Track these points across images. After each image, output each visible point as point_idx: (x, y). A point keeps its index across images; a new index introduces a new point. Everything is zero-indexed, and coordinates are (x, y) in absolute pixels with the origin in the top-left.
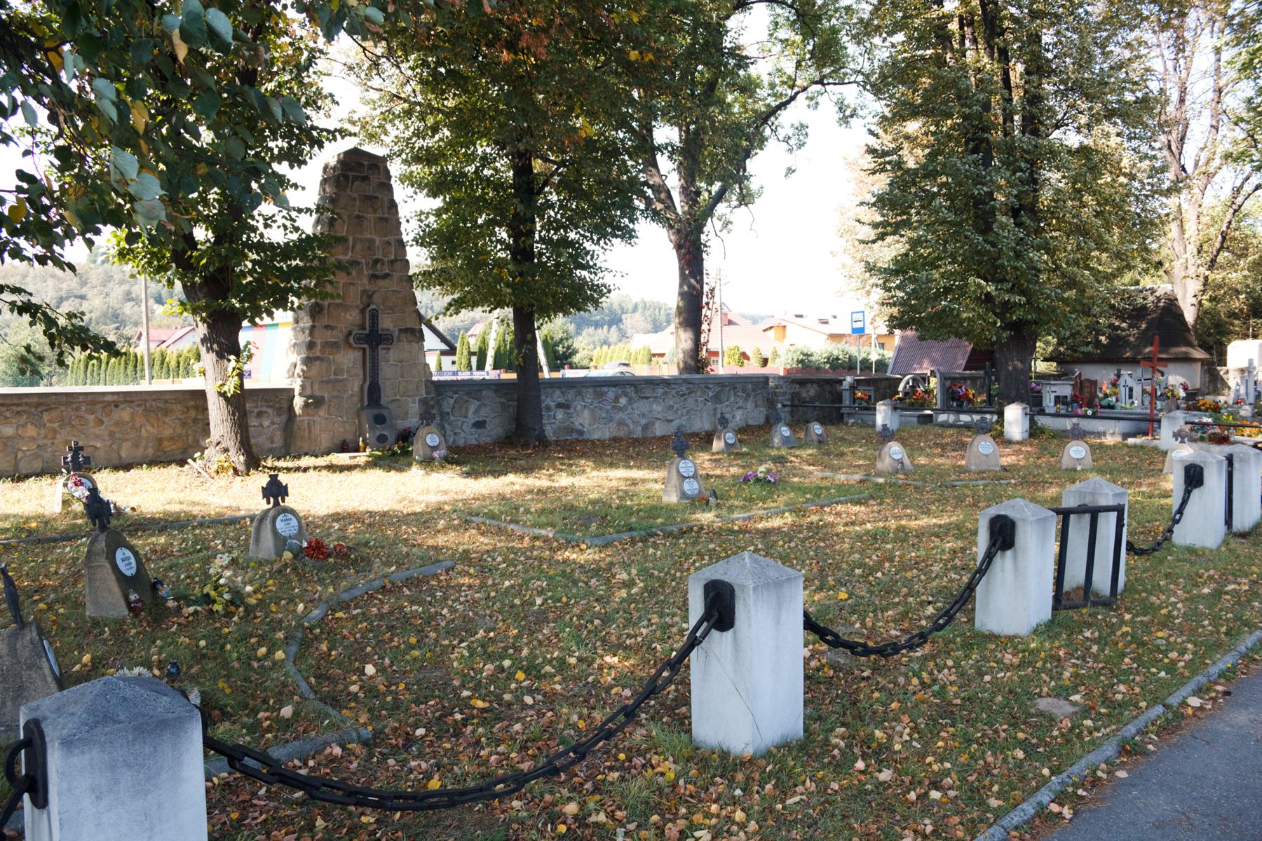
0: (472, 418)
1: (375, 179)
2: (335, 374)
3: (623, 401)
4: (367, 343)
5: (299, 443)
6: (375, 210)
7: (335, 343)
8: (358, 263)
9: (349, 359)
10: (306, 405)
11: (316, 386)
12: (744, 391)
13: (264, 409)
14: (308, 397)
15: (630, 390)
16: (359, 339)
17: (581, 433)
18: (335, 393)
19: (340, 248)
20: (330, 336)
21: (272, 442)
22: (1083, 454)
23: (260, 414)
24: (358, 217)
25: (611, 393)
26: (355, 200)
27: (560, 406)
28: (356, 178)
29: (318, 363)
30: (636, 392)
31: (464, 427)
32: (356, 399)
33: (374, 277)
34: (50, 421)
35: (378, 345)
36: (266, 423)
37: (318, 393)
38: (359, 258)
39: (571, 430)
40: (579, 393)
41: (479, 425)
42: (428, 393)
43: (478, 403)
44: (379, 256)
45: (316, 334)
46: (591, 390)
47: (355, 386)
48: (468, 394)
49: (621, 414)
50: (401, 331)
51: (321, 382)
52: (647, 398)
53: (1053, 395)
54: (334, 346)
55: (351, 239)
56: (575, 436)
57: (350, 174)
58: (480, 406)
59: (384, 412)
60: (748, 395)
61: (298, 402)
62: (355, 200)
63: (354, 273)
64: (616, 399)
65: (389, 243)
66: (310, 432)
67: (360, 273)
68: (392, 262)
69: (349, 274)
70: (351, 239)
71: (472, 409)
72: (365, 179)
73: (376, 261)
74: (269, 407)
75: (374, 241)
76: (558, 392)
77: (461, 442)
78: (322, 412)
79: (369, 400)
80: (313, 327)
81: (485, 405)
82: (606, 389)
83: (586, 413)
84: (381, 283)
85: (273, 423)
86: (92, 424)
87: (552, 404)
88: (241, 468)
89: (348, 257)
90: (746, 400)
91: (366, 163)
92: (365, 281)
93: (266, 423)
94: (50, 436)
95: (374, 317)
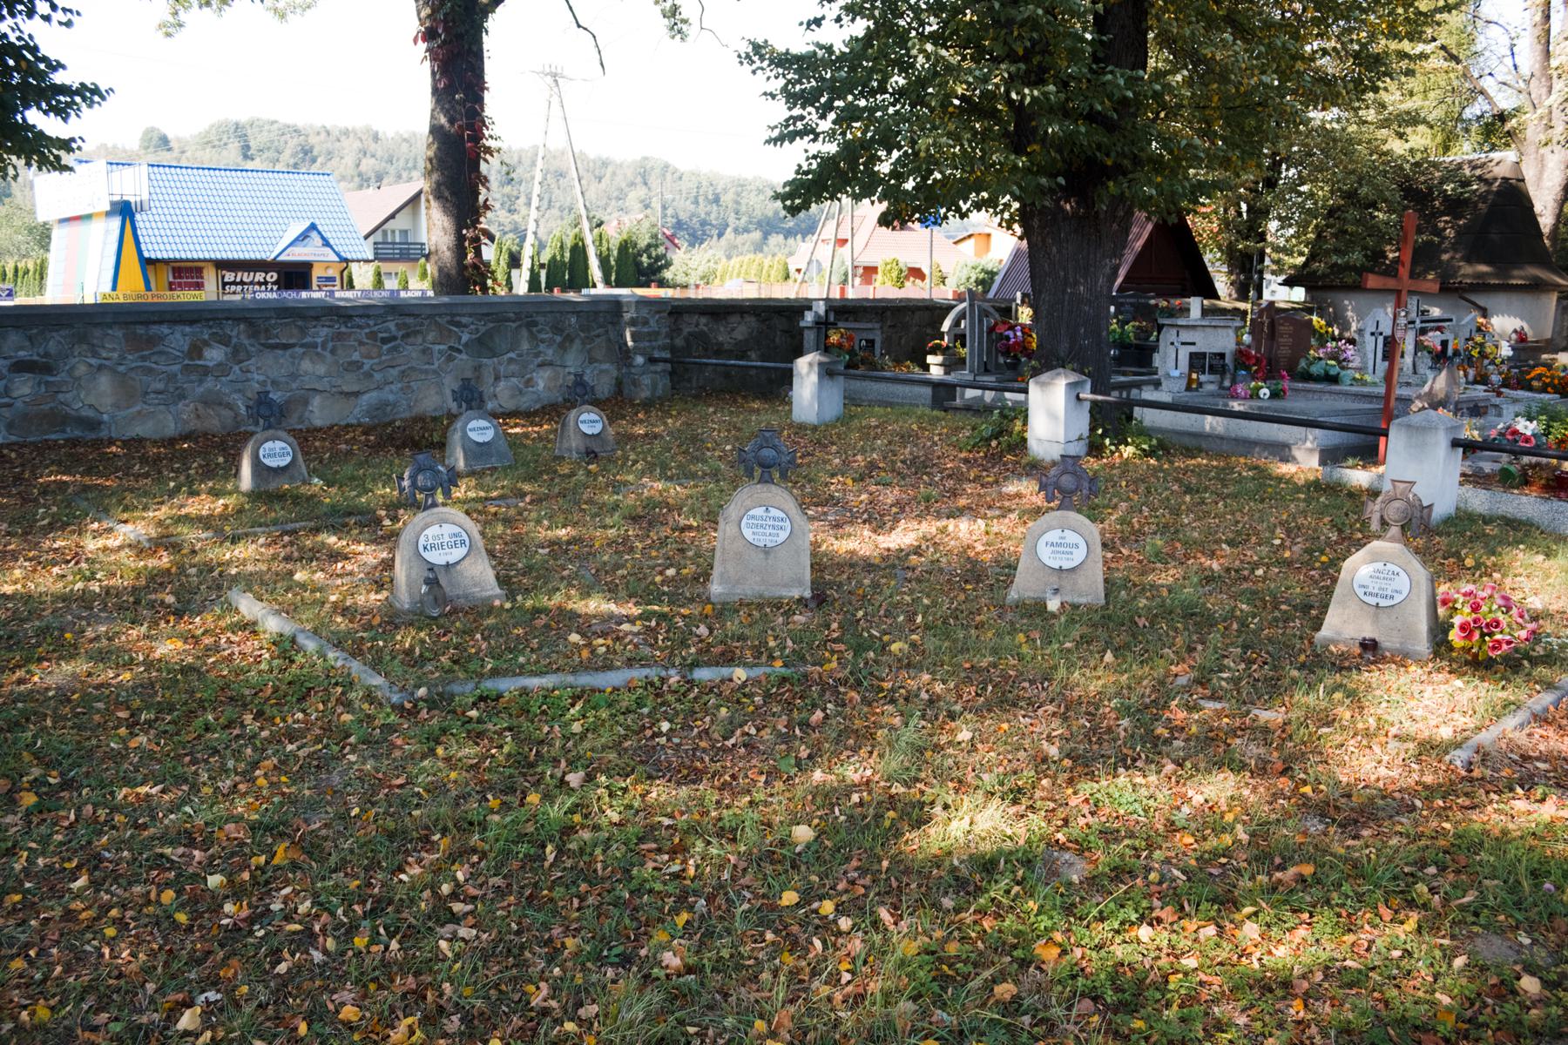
3: (214, 355)
12: (557, 329)
15: (238, 333)
17: (94, 425)
22: (1079, 556)
25: (178, 339)
30: (254, 335)
39: (59, 419)
40: (82, 339)
46: (119, 333)
52: (286, 347)
53: (1184, 353)
56: (74, 432)
60: (569, 339)
64: (196, 351)
82: (165, 329)
83: (104, 382)
90: (563, 347)
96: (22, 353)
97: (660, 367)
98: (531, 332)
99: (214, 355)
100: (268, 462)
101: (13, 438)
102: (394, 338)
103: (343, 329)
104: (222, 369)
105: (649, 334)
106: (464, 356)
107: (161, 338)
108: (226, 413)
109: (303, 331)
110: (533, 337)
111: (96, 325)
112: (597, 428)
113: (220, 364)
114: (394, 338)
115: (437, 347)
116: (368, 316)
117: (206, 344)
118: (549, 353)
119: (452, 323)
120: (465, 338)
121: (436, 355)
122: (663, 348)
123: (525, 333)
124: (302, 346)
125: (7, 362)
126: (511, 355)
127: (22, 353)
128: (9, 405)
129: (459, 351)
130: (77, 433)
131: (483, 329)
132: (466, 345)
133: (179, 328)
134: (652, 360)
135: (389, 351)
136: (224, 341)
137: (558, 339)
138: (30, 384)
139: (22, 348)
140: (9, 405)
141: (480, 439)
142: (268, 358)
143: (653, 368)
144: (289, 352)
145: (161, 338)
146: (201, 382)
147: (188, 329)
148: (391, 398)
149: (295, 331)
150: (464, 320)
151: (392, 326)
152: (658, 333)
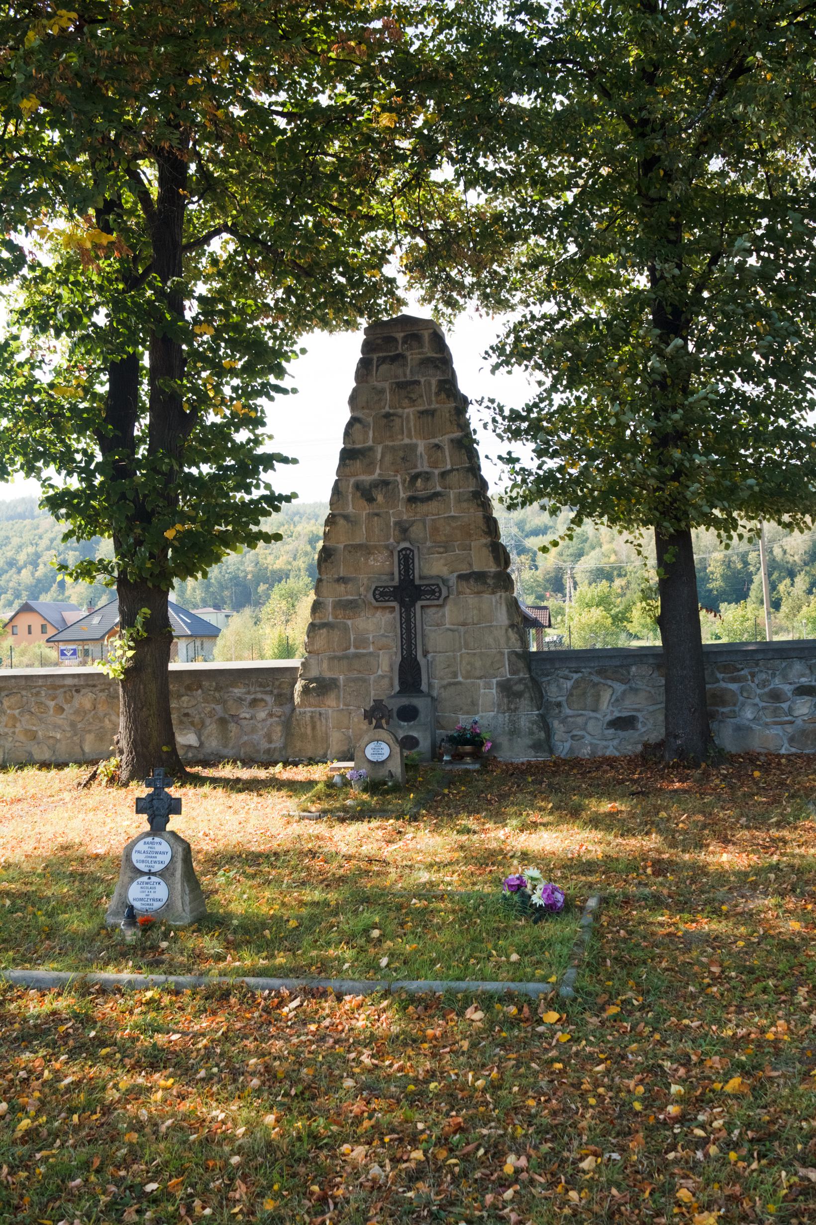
0: (607, 709)
1: (413, 356)
2: (356, 648)
5: (298, 744)
6: (413, 402)
7: (351, 602)
10: (306, 690)
11: (325, 665)
13: (259, 696)
14: (311, 681)
16: (382, 594)
18: (355, 675)
19: (358, 464)
20: (345, 593)
21: (270, 741)
23: (254, 703)
24: (387, 416)
26: (382, 391)
28: (382, 361)
31: (591, 726)
32: (385, 682)
33: (412, 500)
34: (9, 707)
35: (413, 603)
36: (262, 715)
37: (328, 675)
38: (390, 475)
41: (623, 723)
42: (512, 672)
43: (620, 688)
44: (423, 466)
45: (325, 591)
48: (601, 672)
50: (461, 577)
51: (332, 659)
54: (349, 607)
55: (379, 449)
57: (375, 356)
58: (624, 693)
59: (419, 703)
61: (298, 687)
62: (382, 391)
63: (380, 498)
65: (437, 447)
66: (314, 728)
67: (391, 497)
68: (443, 475)
69: (371, 500)
70: (379, 449)
71: (606, 697)
72: (397, 358)
73: (415, 478)
74: (266, 693)
75: (413, 448)
76: (798, 667)
77: (585, 752)
78: (331, 701)
79: (401, 683)
81: (635, 691)
84: (423, 508)
85: (271, 715)
86: (52, 712)
87: (787, 689)
88: (124, 775)
89: (375, 476)
91: (400, 336)
92: (401, 507)
93: (262, 715)
94: (10, 724)
95: (406, 560)
96: (803, 680)
101: (793, 750)
125: (792, 687)
127: (803, 680)
128: (792, 723)
138: (808, 705)
139: (803, 676)
140: (792, 723)
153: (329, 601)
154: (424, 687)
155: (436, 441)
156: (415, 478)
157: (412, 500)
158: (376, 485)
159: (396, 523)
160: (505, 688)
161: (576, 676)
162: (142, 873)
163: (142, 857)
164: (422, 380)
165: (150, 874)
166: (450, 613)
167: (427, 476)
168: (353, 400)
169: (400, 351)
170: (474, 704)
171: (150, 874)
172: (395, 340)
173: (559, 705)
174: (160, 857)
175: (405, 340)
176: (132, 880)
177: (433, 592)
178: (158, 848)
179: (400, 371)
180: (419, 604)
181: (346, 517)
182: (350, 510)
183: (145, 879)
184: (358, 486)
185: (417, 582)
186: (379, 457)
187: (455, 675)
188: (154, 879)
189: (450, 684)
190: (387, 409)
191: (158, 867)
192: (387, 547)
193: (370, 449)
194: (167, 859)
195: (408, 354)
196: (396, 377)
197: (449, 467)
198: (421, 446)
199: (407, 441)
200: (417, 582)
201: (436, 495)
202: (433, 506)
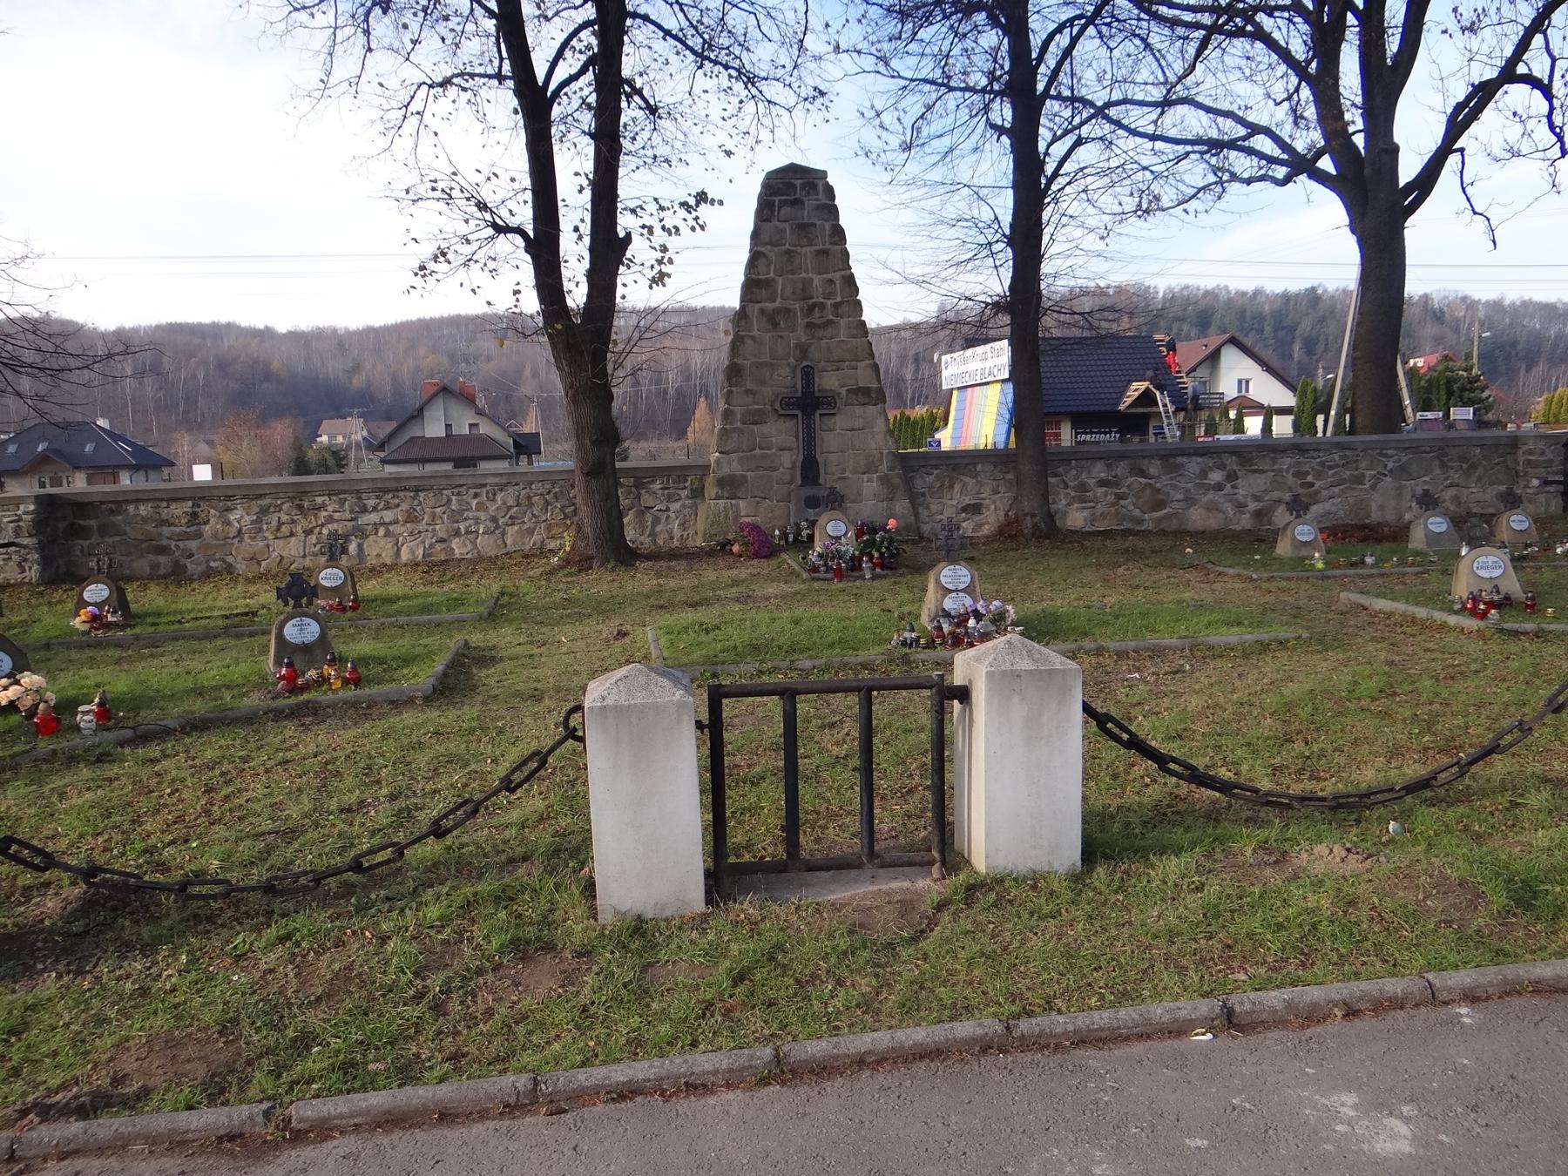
1: (810, 203)
4: (799, 409)
8: (789, 310)
9: (781, 434)
12: (1463, 459)
15: (1232, 463)
19: (764, 293)
24: (788, 252)
25: (1193, 465)
27: (1102, 483)
28: (783, 203)
29: (735, 435)
35: (813, 412)
47: (789, 460)
49: (1211, 495)
52: (1262, 472)
55: (780, 281)
57: (777, 199)
60: (1474, 467)
64: (1204, 474)
65: (831, 281)
68: (836, 306)
72: (797, 203)
73: (811, 308)
79: (803, 478)
80: (730, 392)
82: (1184, 460)
90: (1467, 474)
91: (798, 183)
95: (808, 375)
97: (1552, 488)
98: (1441, 461)
99: (1216, 476)
100: (1299, 538)
102: (1338, 466)
103: (1301, 459)
104: (1219, 487)
105: (1544, 462)
106: (1388, 479)
107: (1182, 466)
108: (1221, 516)
109: (1274, 461)
110: (1443, 465)
111: (1144, 457)
112: (1525, 526)
113: (1218, 483)
114: (1338, 466)
115: (1368, 473)
116: (1319, 450)
117: (1211, 469)
118: (1456, 477)
119: (1381, 454)
120: (1390, 465)
121: (1368, 478)
122: (1557, 473)
123: (1437, 463)
124: (1273, 471)
126: (1427, 478)
129: (1385, 475)
130: (1130, 526)
131: (1404, 459)
132: (1391, 471)
133: (1194, 458)
134: (1546, 483)
135: (1334, 475)
136: (1222, 467)
137: (1465, 466)
141: (1437, 530)
142: (1251, 478)
143: (1547, 489)
144: (1263, 476)
145: (1182, 466)
146: (1205, 494)
147: (1199, 460)
148: (1334, 509)
149: (1268, 461)
150: (1390, 452)
151: (1336, 457)
152: (1551, 461)
153: (738, 410)
154: (821, 481)
155: (829, 276)
156: (811, 308)
157: (809, 325)
158: (777, 311)
159: (797, 345)
160: (884, 480)
161: (935, 472)
162: (951, 591)
163: (949, 580)
164: (818, 223)
165: (956, 591)
166: (841, 421)
167: (822, 306)
168: (755, 236)
169: (798, 196)
170: (859, 494)
171: (956, 591)
172: (795, 186)
173: (923, 494)
174: (963, 579)
175: (804, 186)
176: (944, 596)
177: (829, 404)
178: (960, 573)
179: (800, 213)
180: (819, 412)
181: (753, 338)
182: (755, 332)
183: (954, 594)
184: (762, 311)
185: (817, 394)
186: (780, 288)
187: (844, 471)
188: (961, 594)
189: (840, 478)
190: (787, 246)
191: (962, 586)
192: (788, 365)
193: (773, 280)
194: (968, 579)
195: (805, 199)
196: (796, 219)
197: (839, 299)
198: (817, 280)
199: (804, 275)
200: (817, 394)
201: (830, 322)
202: (829, 331)
